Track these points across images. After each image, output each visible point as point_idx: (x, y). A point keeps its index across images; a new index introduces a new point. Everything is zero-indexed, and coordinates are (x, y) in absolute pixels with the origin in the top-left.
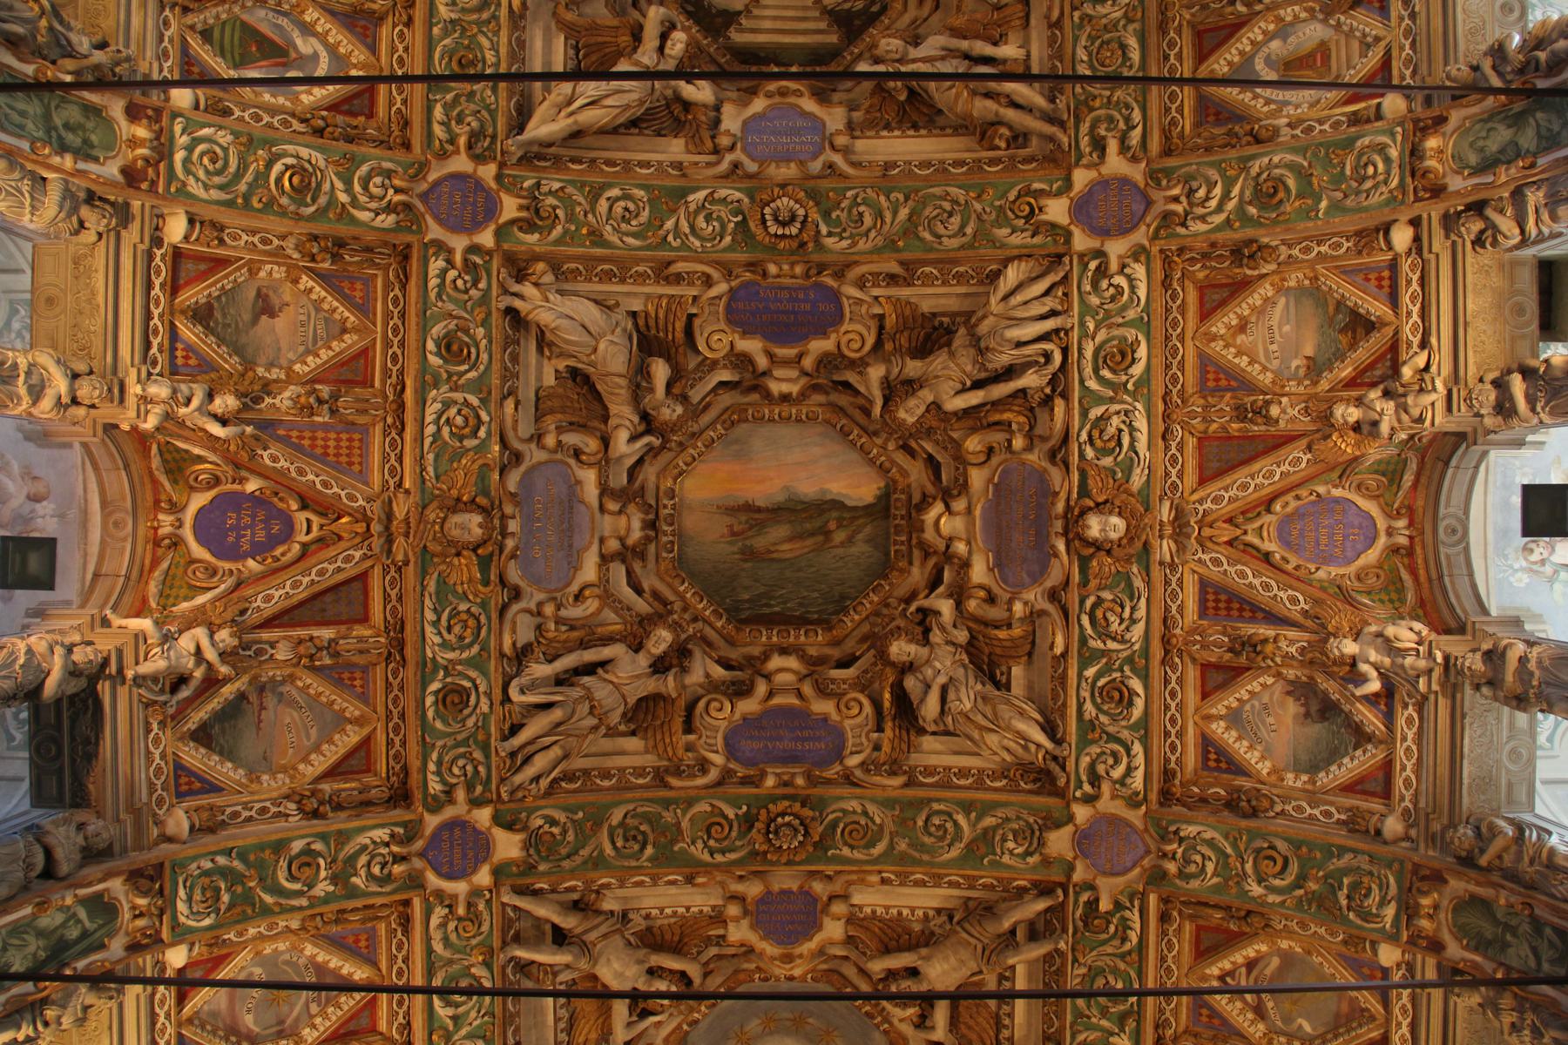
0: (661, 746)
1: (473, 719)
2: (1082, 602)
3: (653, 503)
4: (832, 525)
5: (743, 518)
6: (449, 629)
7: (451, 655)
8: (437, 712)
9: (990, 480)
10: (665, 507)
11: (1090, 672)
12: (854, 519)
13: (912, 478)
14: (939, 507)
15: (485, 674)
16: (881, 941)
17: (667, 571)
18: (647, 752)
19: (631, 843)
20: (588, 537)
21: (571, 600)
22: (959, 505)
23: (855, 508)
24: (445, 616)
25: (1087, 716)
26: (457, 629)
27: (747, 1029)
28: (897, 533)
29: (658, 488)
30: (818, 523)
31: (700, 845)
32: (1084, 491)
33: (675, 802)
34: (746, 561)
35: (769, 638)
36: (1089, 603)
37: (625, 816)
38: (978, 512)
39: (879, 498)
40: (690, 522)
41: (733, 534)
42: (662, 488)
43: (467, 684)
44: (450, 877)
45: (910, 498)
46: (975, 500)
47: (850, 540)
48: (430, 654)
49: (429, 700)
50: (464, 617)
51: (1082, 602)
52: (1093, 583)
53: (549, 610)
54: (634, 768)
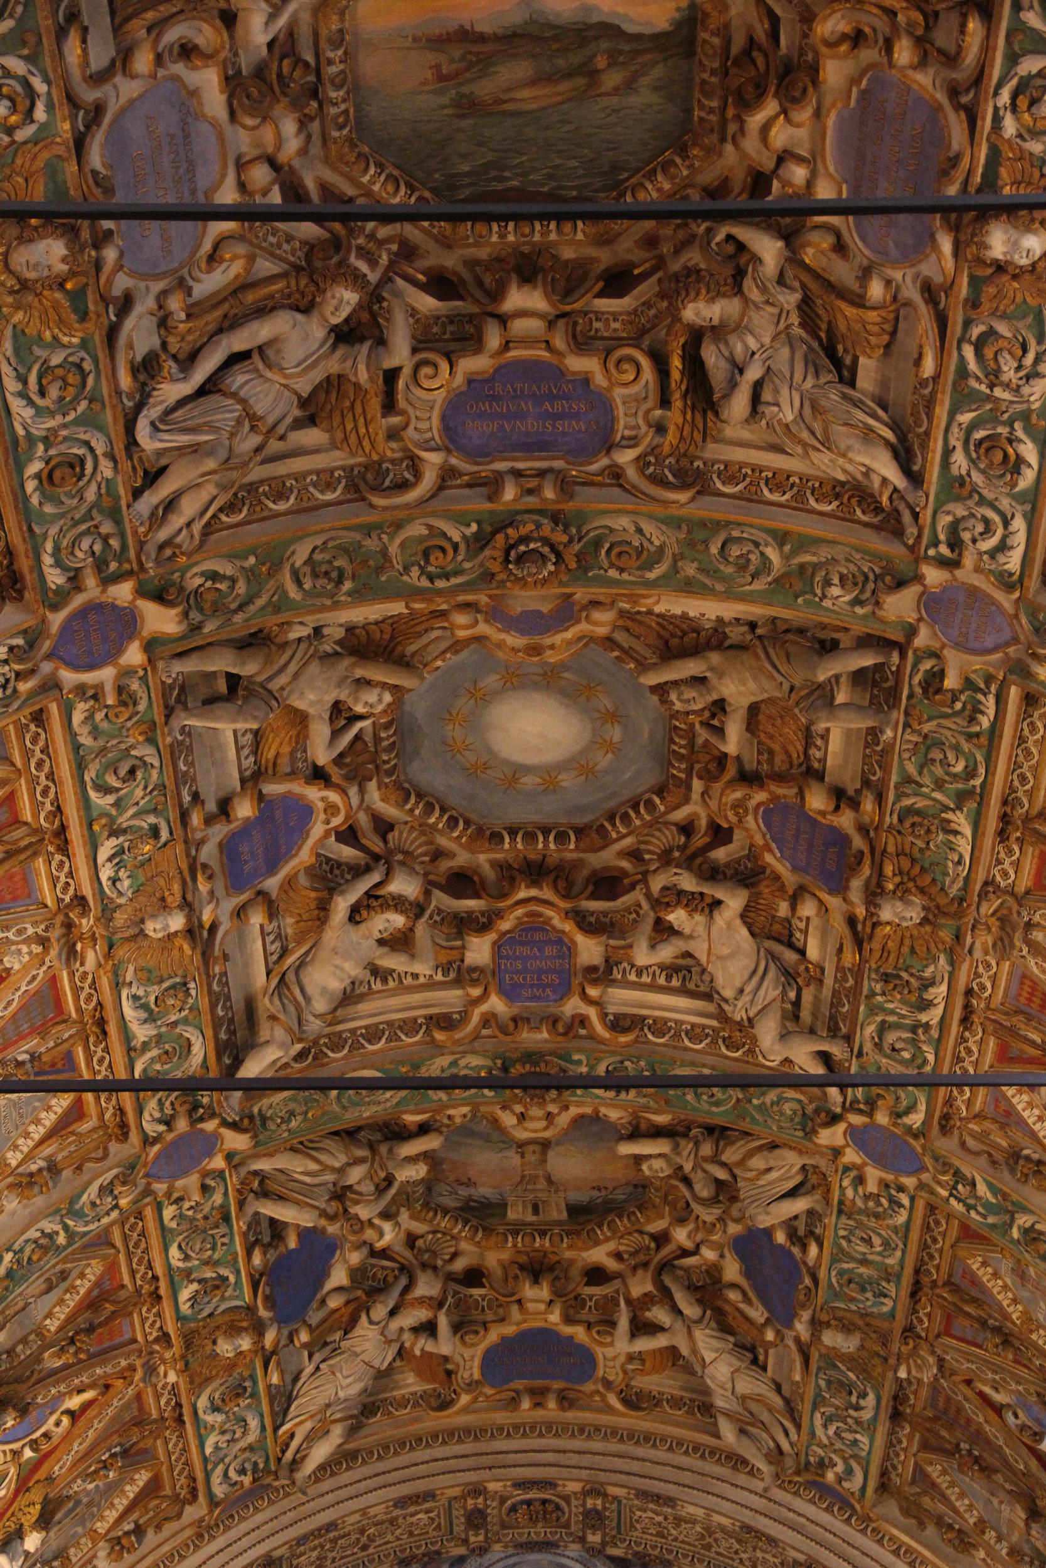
0: (353, 439)
1: (93, 488)
2: (967, 323)
3: (309, 58)
4: (601, 62)
5: (457, 53)
6: (42, 393)
7: (52, 423)
8: (43, 494)
9: (854, 81)
10: (330, 62)
11: (966, 418)
12: (637, 53)
13: (733, 12)
14: (771, 107)
15: (101, 428)
16: (660, 636)
17: (341, 158)
18: (334, 446)
19: (323, 581)
20: (217, 166)
21: (203, 265)
22: (804, 115)
23: (638, 37)
24: (33, 379)
25: (954, 470)
26: (54, 392)
27: (482, 684)
28: (707, 94)
29: (316, 35)
30: (576, 59)
31: (415, 572)
32: (990, 180)
33: (378, 527)
34: (463, 116)
35: (502, 236)
36: (976, 331)
37: (313, 551)
38: (831, 121)
39: (678, 25)
40: (369, 66)
41: (442, 78)
42: (324, 32)
43: (81, 451)
44: (91, 667)
45: (727, 42)
46: (828, 101)
47: (629, 85)
48: (21, 432)
49: (30, 486)
50: (60, 372)
51: (967, 323)
52: (986, 306)
53: (175, 304)
54: (318, 472)
